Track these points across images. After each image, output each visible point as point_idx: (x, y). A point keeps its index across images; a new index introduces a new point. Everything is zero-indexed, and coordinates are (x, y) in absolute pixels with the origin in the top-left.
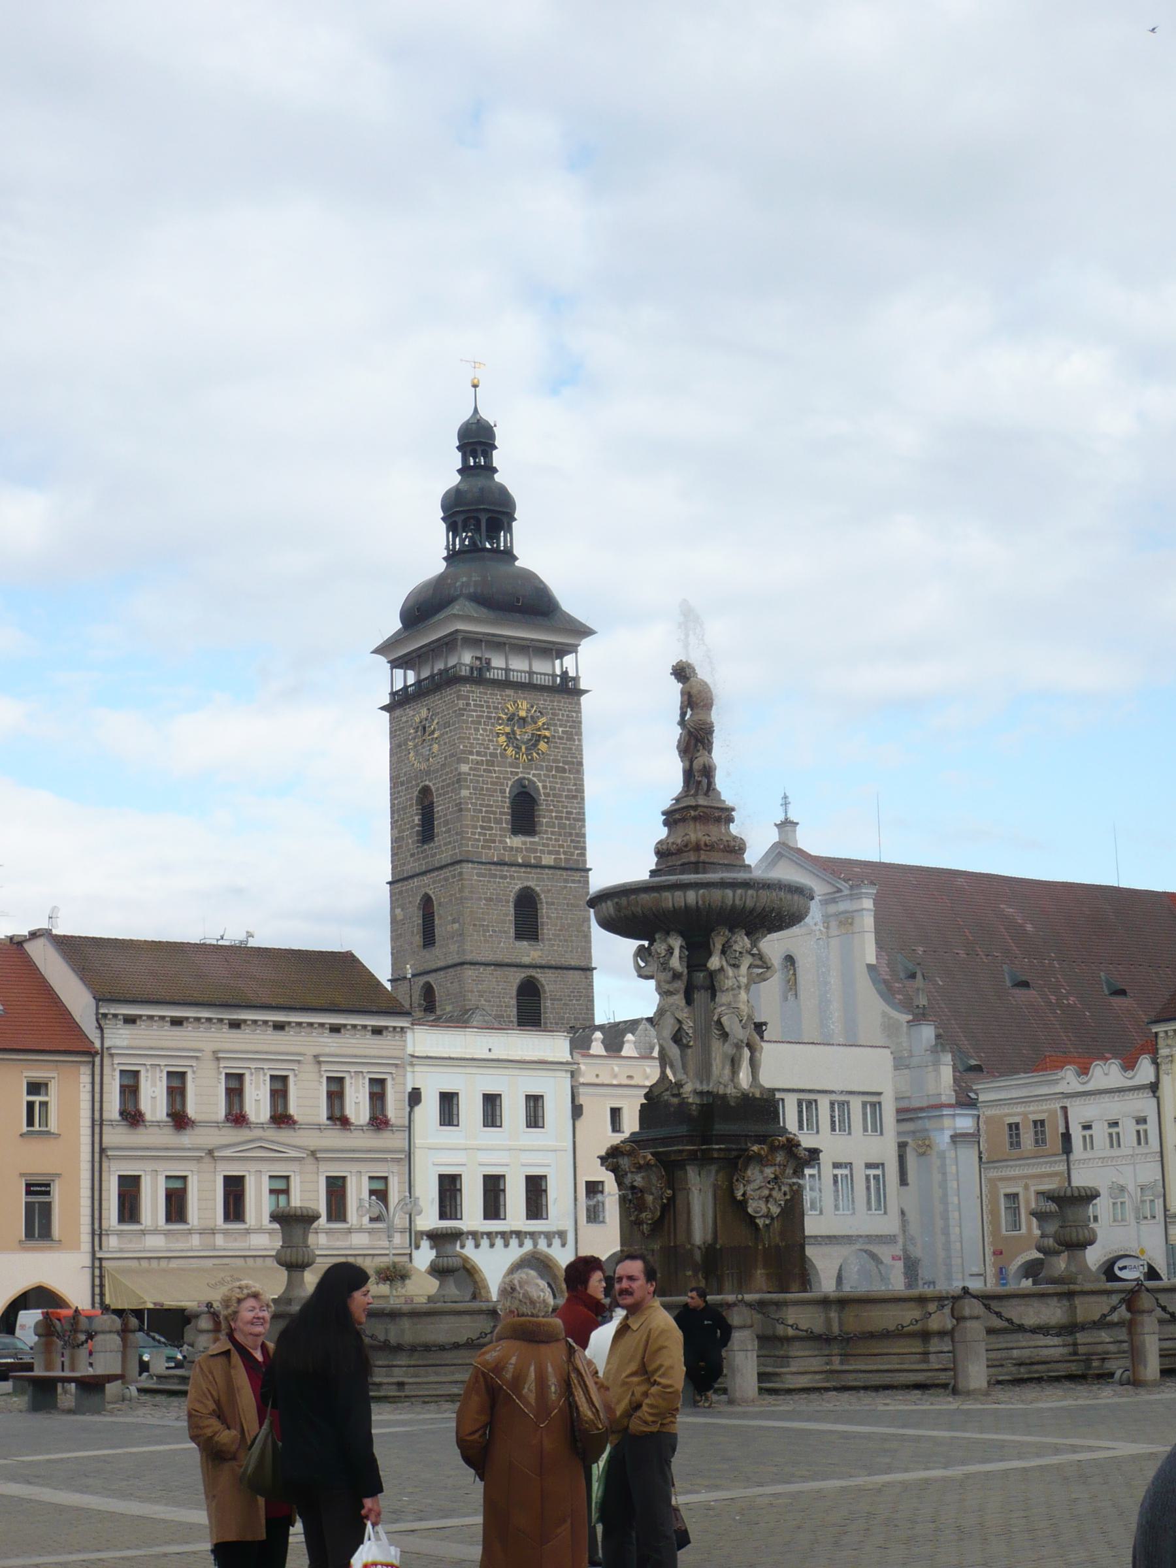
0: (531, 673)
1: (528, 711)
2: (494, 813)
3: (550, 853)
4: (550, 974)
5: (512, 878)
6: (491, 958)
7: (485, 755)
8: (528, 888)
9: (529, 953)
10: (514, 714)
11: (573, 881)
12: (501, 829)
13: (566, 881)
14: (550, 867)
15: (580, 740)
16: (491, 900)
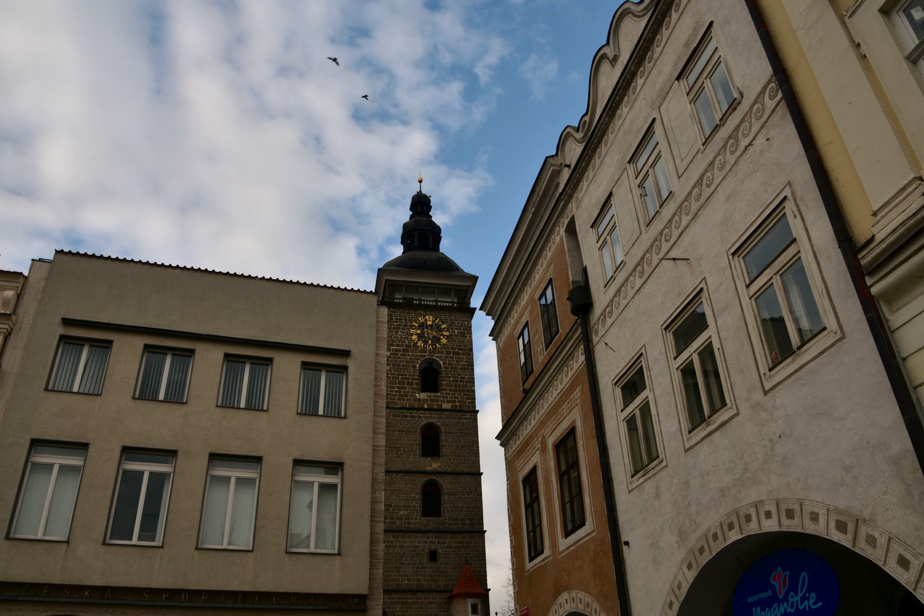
0: (437, 301)
1: (433, 321)
2: (408, 379)
3: (448, 402)
4: (448, 478)
5: (419, 417)
6: (401, 467)
7: (402, 346)
8: (432, 423)
9: (435, 465)
10: (423, 323)
11: (466, 419)
12: (412, 388)
13: (460, 419)
14: (447, 410)
15: (471, 337)
16: (403, 431)
